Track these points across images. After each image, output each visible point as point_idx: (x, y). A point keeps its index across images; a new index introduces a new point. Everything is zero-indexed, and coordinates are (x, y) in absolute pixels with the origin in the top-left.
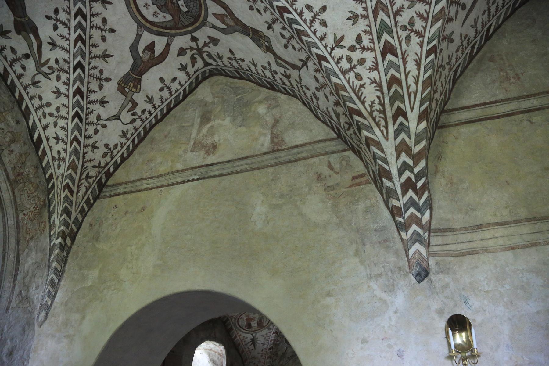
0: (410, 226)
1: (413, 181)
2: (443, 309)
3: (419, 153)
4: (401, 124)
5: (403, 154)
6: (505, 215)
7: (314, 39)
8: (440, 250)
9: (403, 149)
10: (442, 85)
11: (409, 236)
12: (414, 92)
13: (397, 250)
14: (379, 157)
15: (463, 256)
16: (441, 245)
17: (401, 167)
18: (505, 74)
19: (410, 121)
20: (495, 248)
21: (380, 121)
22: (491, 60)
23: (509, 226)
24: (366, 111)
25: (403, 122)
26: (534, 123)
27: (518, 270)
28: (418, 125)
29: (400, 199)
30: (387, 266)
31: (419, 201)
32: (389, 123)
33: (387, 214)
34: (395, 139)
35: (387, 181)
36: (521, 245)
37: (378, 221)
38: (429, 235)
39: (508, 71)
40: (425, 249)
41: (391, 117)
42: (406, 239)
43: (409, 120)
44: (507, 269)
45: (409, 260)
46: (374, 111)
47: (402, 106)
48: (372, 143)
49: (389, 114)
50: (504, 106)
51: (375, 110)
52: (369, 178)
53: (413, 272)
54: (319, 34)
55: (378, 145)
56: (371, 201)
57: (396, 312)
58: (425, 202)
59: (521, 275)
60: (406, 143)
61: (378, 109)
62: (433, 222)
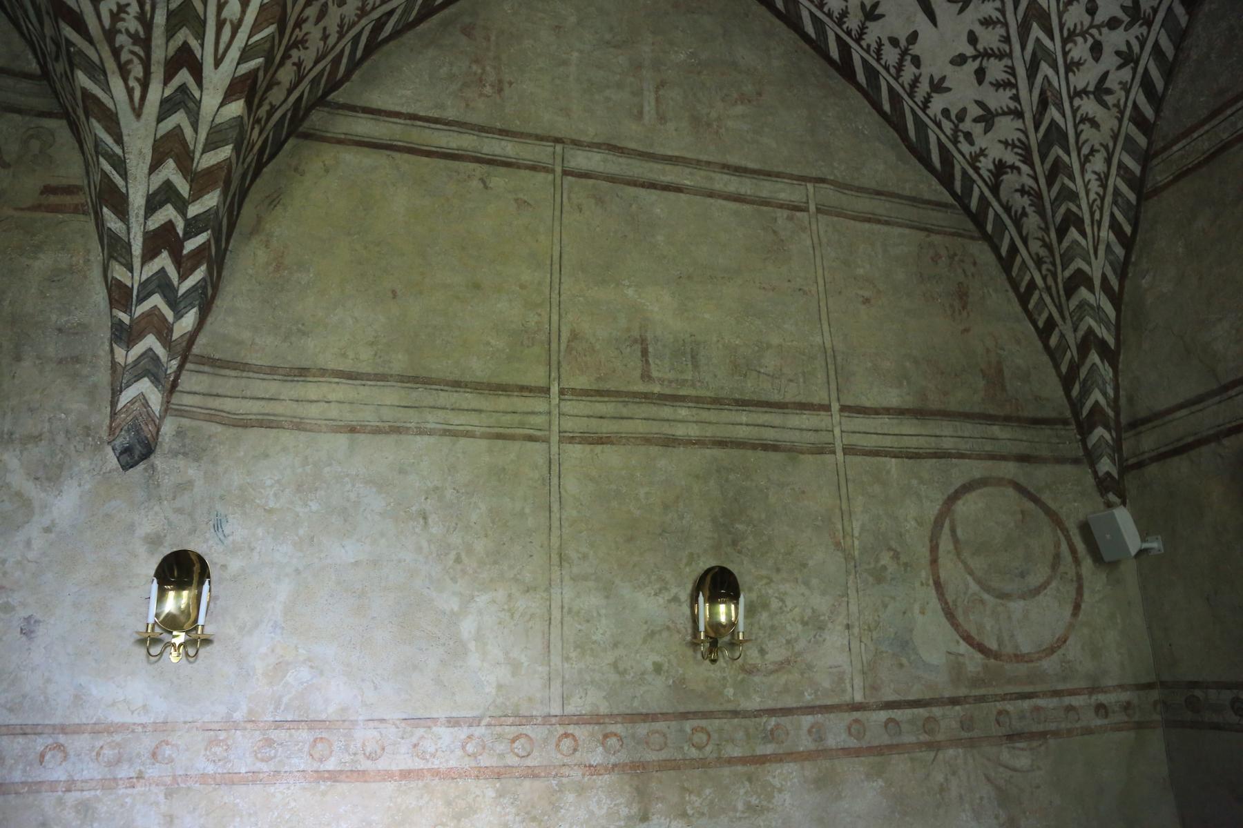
0: (141, 336)
1: (178, 234)
2: (162, 535)
3: (209, 171)
4: (183, 88)
5: (171, 164)
6: (364, 360)
8: (196, 405)
9: (171, 150)
10: (325, 37)
11: (130, 360)
12: (231, 22)
13: (95, 386)
14: (107, 152)
15: (245, 426)
16: (204, 395)
17: (156, 193)
18: (480, 71)
19: (208, 89)
20: (319, 422)
21: (130, 62)
22: (467, 31)
23: (363, 382)
24: (97, 21)
25: (188, 85)
26: (491, 188)
27: (348, 475)
28: (222, 105)
29: (135, 267)
30: (60, 419)
31: (179, 284)
32: (153, 76)
33: (99, 296)
34: (160, 120)
35: (113, 215)
36: (372, 426)
37: (73, 308)
38: (181, 367)
39: (488, 68)
40: (160, 396)
41: (162, 61)
42: (123, 365)
43: (205, 86)
44: (327, 469)
45: (114, 414)
46: (120, 31)
47: (194, 44)
48: (96, 111)
49: (160, 52)
50: (450, 136)
51: (123, 30)
52: (86, 201)
53: (117, 442)
55: (111, 121)
56: (72, 257)
57: (47, 530)
58: (193, 289)
59: (349, 486)
60: (185, 139)
61: (132, 31)
62: (201, 340)
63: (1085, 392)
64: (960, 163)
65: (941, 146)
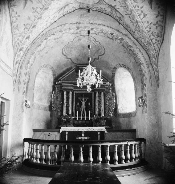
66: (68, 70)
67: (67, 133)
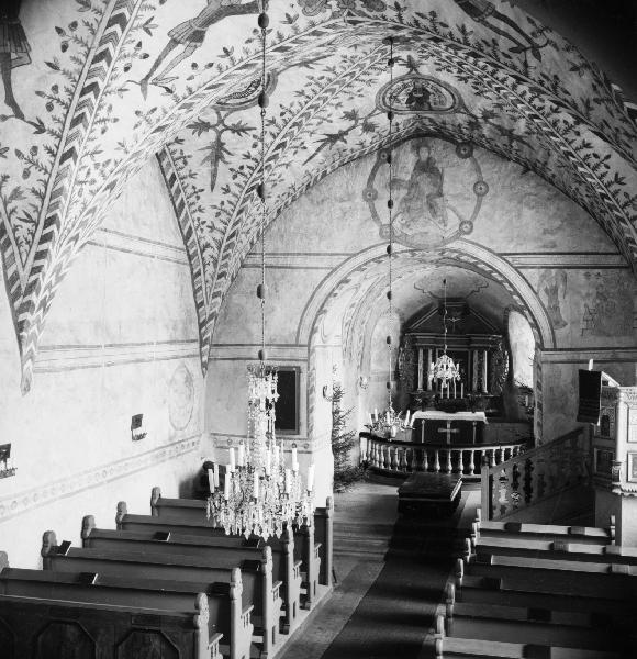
7: (85, 134)
54: (92, 135)
63: (205, 333)
64: (194, 237)
65: (190, 228)
66: (426, 309)
67: (423, 422)
